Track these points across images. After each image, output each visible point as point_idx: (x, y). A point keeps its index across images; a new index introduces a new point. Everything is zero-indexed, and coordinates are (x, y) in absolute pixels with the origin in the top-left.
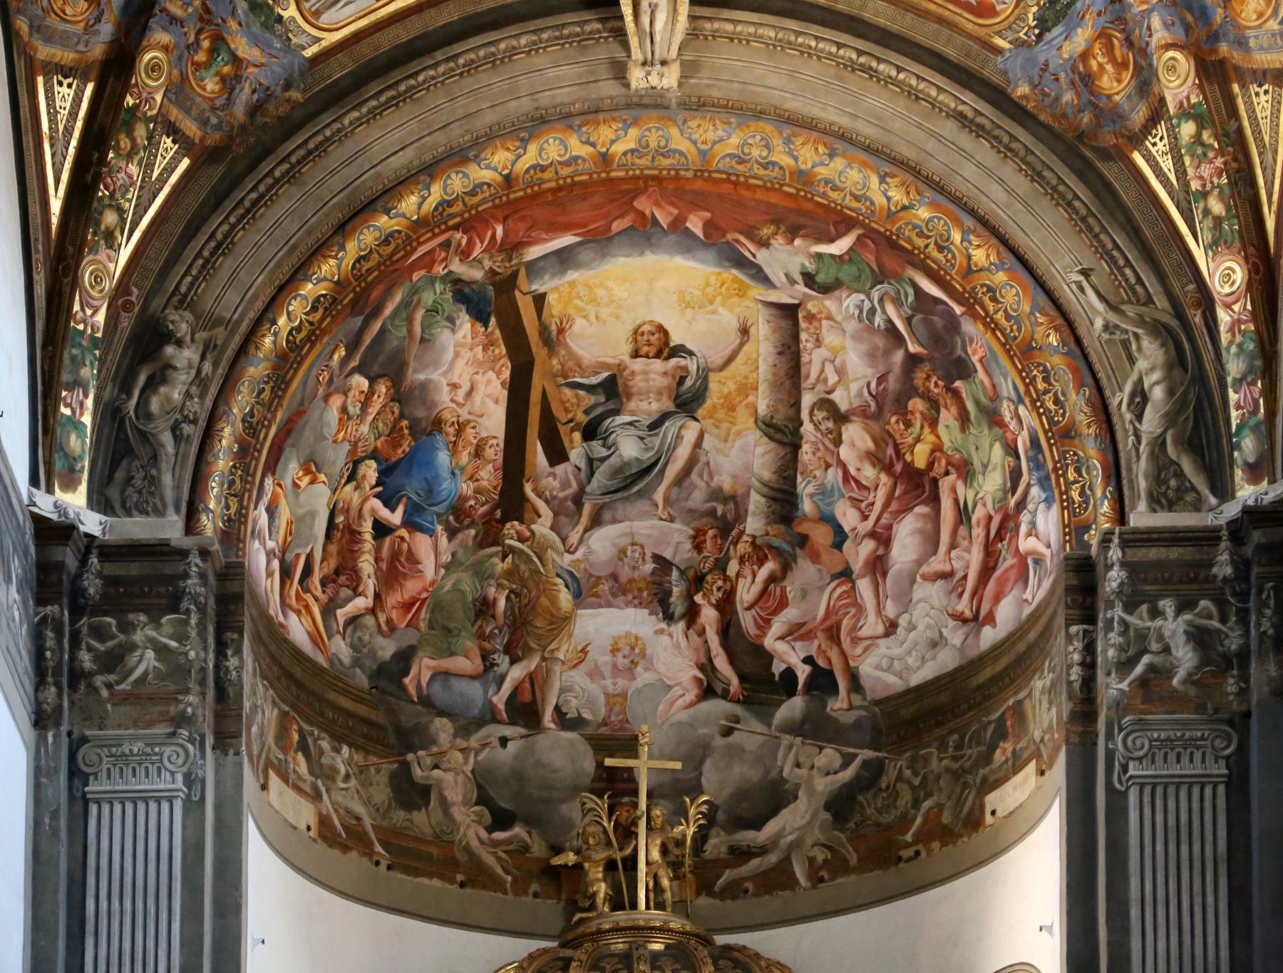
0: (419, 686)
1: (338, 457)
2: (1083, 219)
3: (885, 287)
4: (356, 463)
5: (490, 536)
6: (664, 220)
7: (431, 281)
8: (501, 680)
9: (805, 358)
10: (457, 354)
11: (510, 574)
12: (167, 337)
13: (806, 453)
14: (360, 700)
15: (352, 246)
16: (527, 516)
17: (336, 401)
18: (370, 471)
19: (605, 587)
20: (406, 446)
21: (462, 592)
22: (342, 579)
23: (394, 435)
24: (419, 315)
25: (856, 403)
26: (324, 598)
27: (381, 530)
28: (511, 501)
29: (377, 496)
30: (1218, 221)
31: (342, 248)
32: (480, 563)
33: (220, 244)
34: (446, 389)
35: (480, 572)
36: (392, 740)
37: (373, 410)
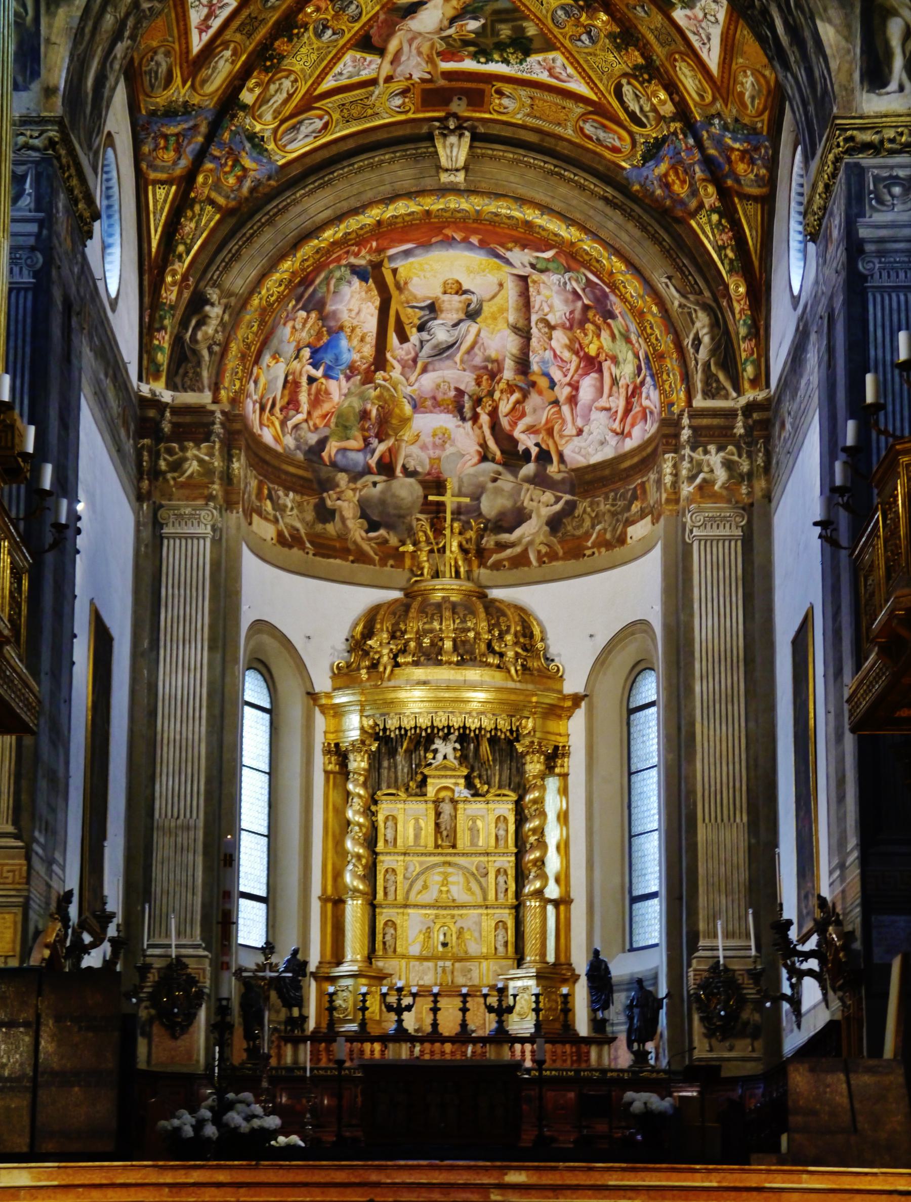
0: (330, 456)
1: (290, 349)
2: (668, 251)
3: (571, 274)
4: (299, 350)
5: (368, 379)
6: (458, 236)
7: (339, 267)
8: (373, 452)
9: (532, 299)
10: (352, 297)
11: (379, 397)
12: (207, 302)
13: (534, 342)
14: (299, 467)
15: (299, 255)
16: (388, 368)
17: (290, 324)
18: (306, 353)
19: (429, 403)
20: (325, 339)
21: (353, 408)
22: (291, 406)
23: (319, 335)
24: (333, 282)
25: (559, 322)
26: (281, 417)
27: (311, 380)
28: (380, 361)
29: (310, 364)
30: (731, 261)
31: (295, 256)
32: (363, 392)
33: (234, 255)
34: (346, 312)
35: (363, 397)
36: (315, 486)
37: (308, 326)
